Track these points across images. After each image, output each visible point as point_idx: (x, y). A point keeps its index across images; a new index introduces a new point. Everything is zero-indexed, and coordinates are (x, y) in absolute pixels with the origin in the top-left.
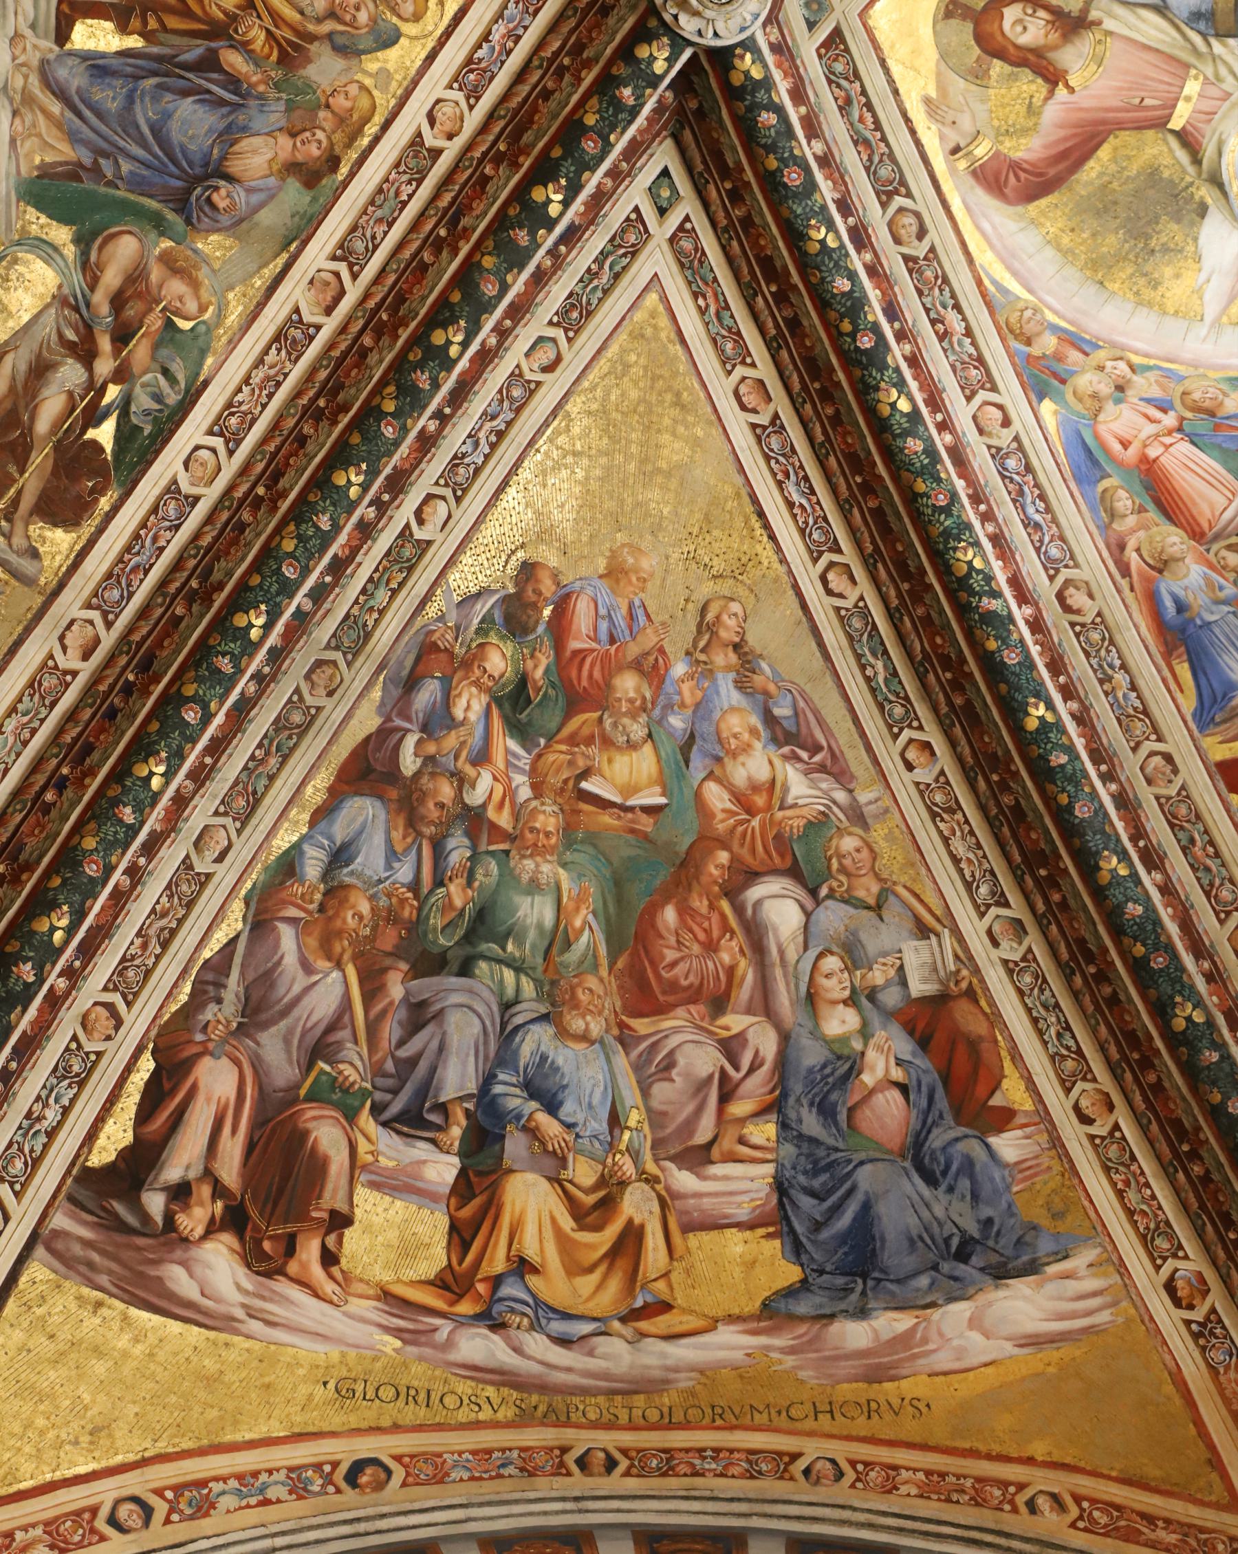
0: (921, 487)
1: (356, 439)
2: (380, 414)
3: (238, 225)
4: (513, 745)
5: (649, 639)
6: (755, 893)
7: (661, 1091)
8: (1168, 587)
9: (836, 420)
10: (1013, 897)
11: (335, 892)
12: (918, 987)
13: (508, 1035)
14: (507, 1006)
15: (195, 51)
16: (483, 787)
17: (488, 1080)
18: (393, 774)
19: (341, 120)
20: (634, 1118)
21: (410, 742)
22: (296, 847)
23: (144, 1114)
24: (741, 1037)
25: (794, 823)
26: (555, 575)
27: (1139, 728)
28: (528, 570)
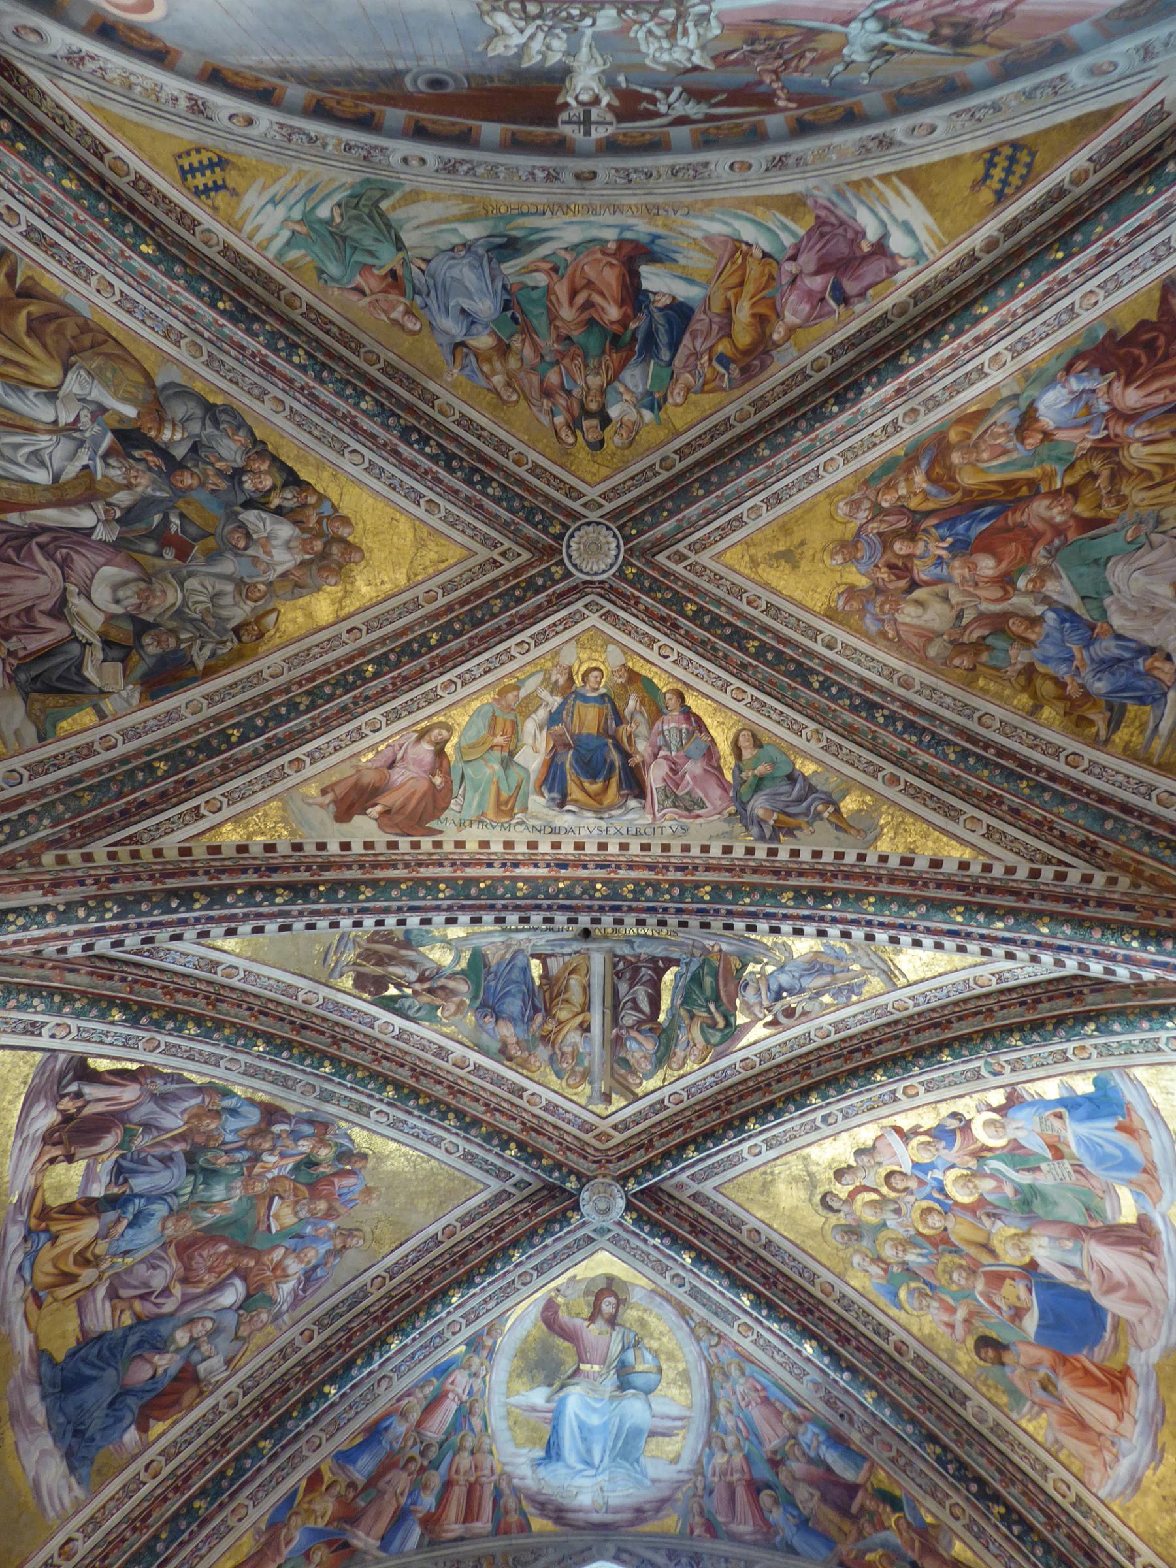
0: (422, 1314)
1: (406, 1091)
2: (417, 1098)
3: (480, 1027)
4: (290, 1166)
5: (342, 1210)
6: (238, 1282)
7: (142, 1268)
8: (395, 1420)
9: (444, 1269)
10: (249, 1398)
11: (217, 1114)
12: (202, 1368)
13: (161, 1198)
14: (175, 1193)
15: (540, 1005)
16: (270, 1159)
17: (140, 1196)
18: (271, 1123)
19: (526, 1060)
20: (129, 1260)
22: (235, 1095)
23: (111, 1072)
24: (171, 1295)
25: (270, 1291)
26: (364, 1167)
27: (331, 1429)
28: (364, 1157)
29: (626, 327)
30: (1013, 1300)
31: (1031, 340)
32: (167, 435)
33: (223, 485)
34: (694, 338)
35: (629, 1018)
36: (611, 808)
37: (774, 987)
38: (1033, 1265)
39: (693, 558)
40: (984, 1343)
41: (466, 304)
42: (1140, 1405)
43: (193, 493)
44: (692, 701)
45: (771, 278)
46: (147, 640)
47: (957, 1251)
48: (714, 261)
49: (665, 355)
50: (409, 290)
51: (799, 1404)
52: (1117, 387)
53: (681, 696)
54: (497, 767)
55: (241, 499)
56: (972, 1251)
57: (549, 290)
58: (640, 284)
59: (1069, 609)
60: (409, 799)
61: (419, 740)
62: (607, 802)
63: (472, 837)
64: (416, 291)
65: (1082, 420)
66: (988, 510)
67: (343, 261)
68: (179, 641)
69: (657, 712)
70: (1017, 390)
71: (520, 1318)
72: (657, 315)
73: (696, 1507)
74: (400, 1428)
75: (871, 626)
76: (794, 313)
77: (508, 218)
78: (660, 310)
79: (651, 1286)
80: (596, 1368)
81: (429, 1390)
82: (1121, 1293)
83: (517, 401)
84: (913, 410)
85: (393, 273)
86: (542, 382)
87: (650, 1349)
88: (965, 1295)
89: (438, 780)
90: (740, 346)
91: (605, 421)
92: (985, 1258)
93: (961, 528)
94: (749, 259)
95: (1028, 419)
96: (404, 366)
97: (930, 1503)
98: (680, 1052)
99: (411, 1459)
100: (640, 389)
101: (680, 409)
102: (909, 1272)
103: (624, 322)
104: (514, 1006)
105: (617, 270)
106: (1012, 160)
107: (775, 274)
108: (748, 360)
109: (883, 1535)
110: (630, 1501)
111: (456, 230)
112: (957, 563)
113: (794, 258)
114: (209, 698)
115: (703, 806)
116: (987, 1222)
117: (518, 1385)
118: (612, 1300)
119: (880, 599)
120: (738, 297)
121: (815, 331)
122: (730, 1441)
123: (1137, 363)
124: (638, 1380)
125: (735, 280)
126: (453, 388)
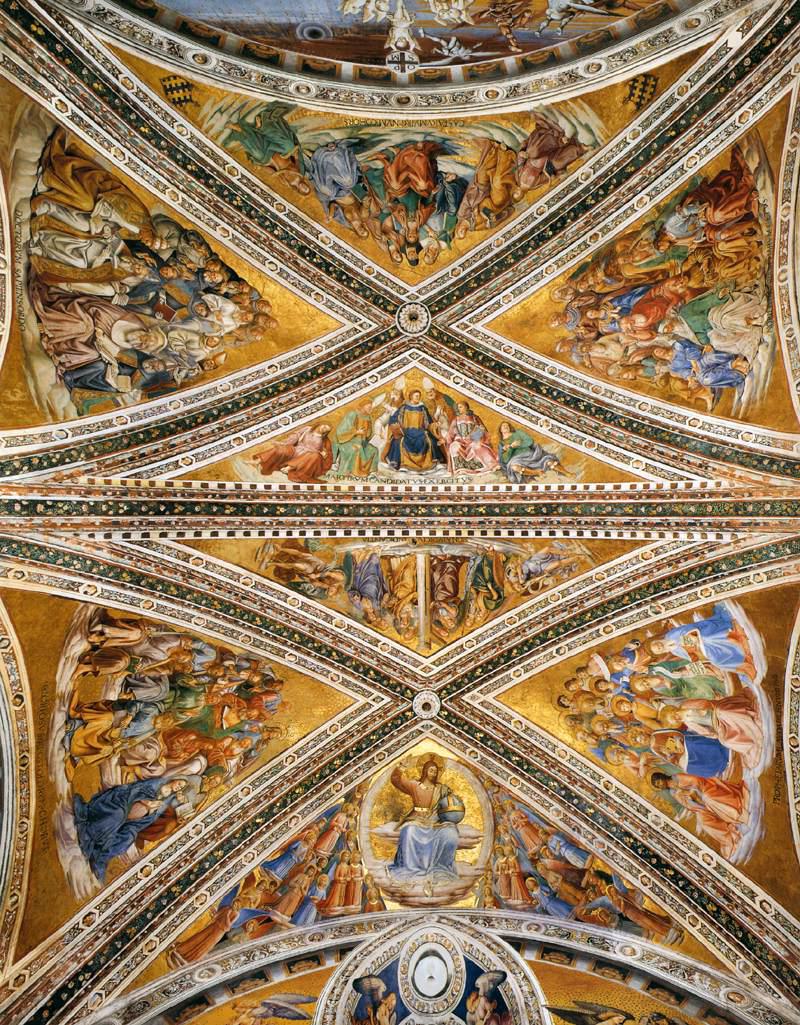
5: (268, 715)
11: (190, 652)
15: (387, 589)
18: (222, 660)
19: (379, 623)
21: (232, 663)
30: (673, 750)
31: (660, 188)
32: (157, 245)
33: (193, 278)
35: (440, 596)
36: (427, 469)
37: (526, 571)
38: (683, 728)
39: (472, 326)
40: (657, 776)
42: (751, 802)
43: (174, 282)
44: (473, 407)
45: (512, 162)
46: (146, 365)
47: (639, 724)
49: (453, 209)
51: (548, 824)
52: (710, 211)
53: (467, 405)
54: (359, 446)
55: (203, 287)
56: (648, 723)
57: (384, 171)
59: (688, 340)
60: (306, 464)
61: (312, 430)
62: (424, 465)
63: (345, 486)
64: (306, 170)
65: (691, 233)
66: (640, 289)
67: (264, 152)
68: (166, 367)
69: (453, 415)
70: (653, 218)
71: (378, 780)
73: (487, 891)
74: (304, 848)
75: (575, 359)
76: (526, 183)
77: (359, 127)
79: (457, 759)
80: (425, 810)
81: (321, 825)
82: (737, 737)
84: (595, 234)
85: (292, 158)
87: (457, 797)
88: (647, 749)
89: (324, 454)
91: (419, 248)
92: (655, 726)
93: (625, 301)
95: (660, 235)
97: (628, 876)
98: (472, 616)
99: (311, 867)
100: (439, 229)
102: (611, 740)
103: (428, 191)
104: (372, 588)
105: (423, 160)
106: (645, 84)
109: (600, 900)
110: (446, 889)
112: (623, 321)
113: (524, 149)
114: (184, 400)
115: (481, 466)
116: (655, 704)
117: (380, 822)
118: (434, 768)
119: (580, 344)
120: (493, 174)
121: (538, 192)
122: (507, 849)
123: (721, 196)
124: (451, 816)
125: (491, 164)
126: (328, 227)
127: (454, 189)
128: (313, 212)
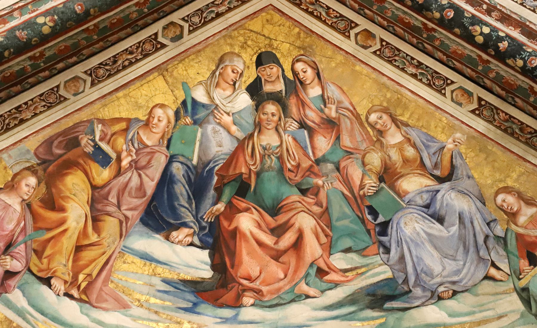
29: (230, 205)
34: (141, 188)
41: (436, 228)
45: (39, 254)
48: (115, 277)
49: (178, 169)
50: (512, 243)
58: (210, 256)
64: (503, 241)
72: (189, 218)
78: (185, 225)
83: (369, 113)
86: (338, 138)
90: (80, 173)
94: (68, 278)
96: (518, 148)
100: (210, 128)
101: (158, 101)
105: (242, 272)
107: (34, 257)
108: (70, 155)
111: (450, 315)
120: (84, 233)
125: (87, 255)
127: (174, 211)
128: (488, 154)
